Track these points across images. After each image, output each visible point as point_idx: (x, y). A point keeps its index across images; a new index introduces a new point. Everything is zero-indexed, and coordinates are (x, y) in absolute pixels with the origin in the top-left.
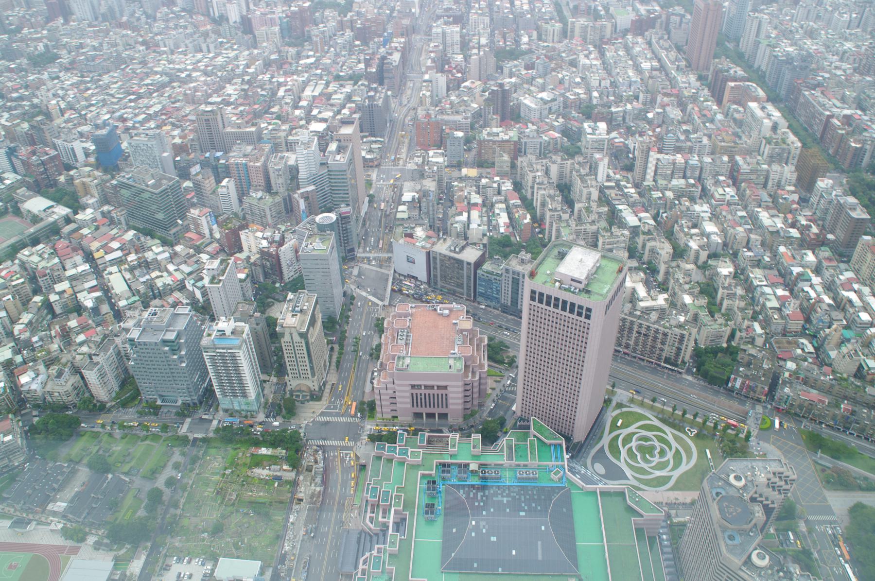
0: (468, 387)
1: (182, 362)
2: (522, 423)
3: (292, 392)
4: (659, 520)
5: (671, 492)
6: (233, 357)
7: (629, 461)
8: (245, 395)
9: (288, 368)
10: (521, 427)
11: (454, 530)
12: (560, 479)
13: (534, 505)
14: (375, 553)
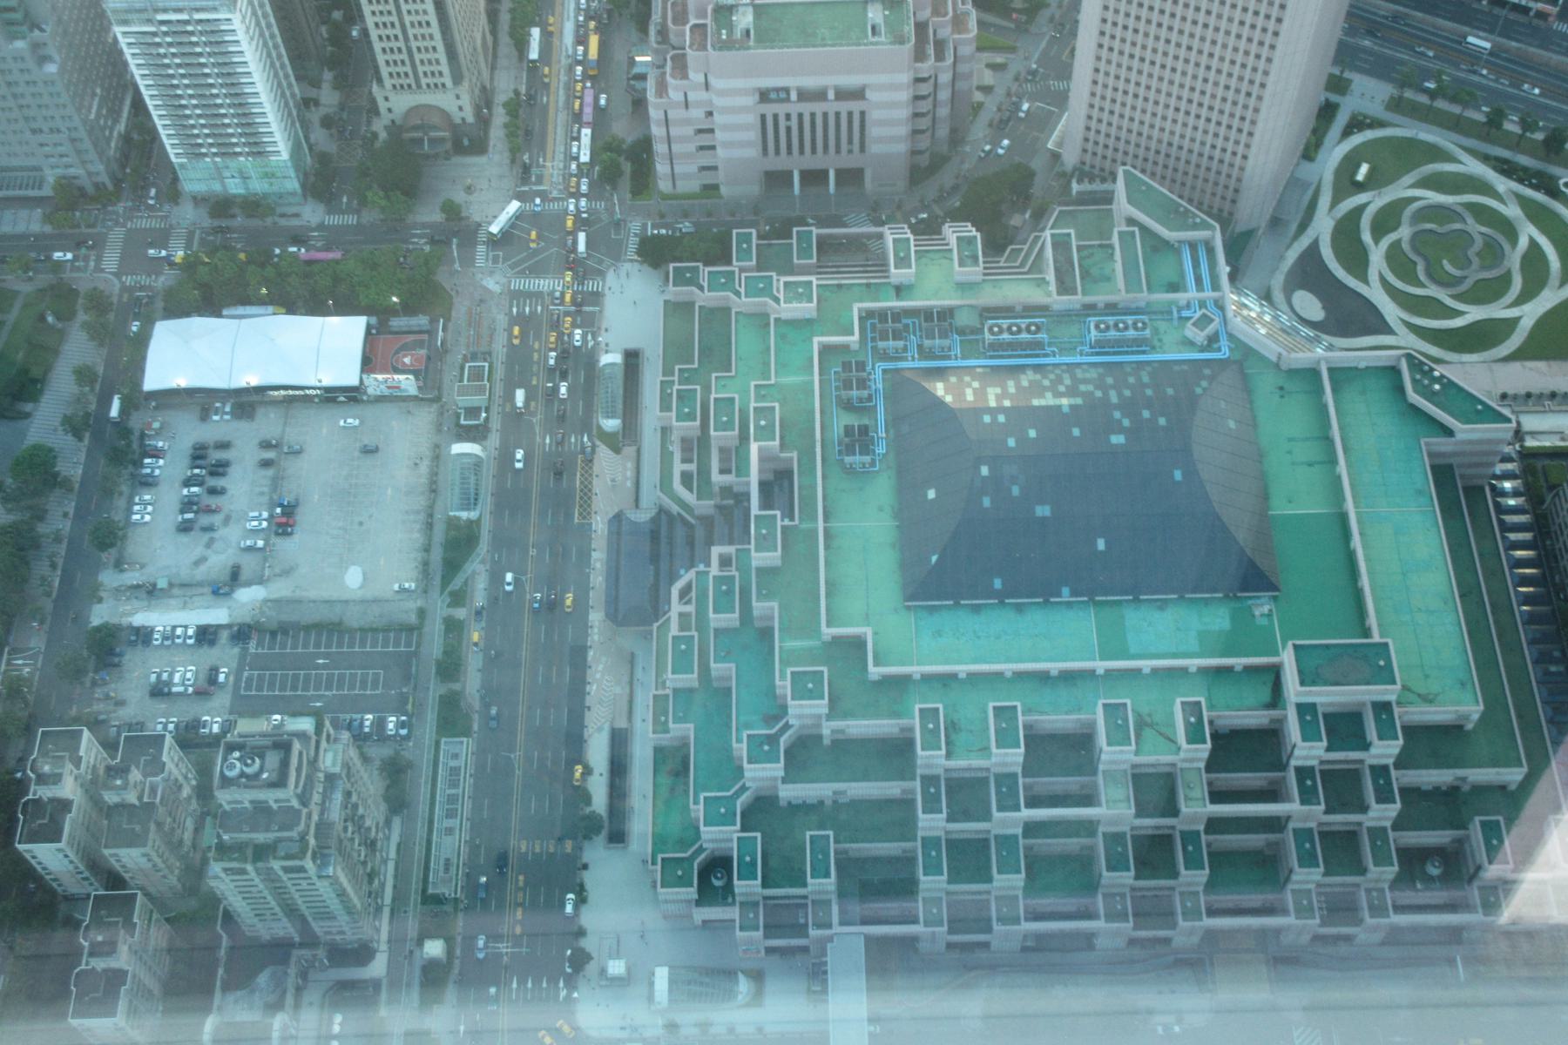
0: (925, 89)
1: (43, 60)
2: (1087, 186)
3: (395, 129)
4: (1500, 441)
5: (1516, 366)
6: (216, 37)
7: (1391, 278)
8: (258, 149)
9: (381, 59)
10: (1085, 199)
11: (931, 494)
12: (1213, 339)
13: (1146, 414)
14: (714, 570)
